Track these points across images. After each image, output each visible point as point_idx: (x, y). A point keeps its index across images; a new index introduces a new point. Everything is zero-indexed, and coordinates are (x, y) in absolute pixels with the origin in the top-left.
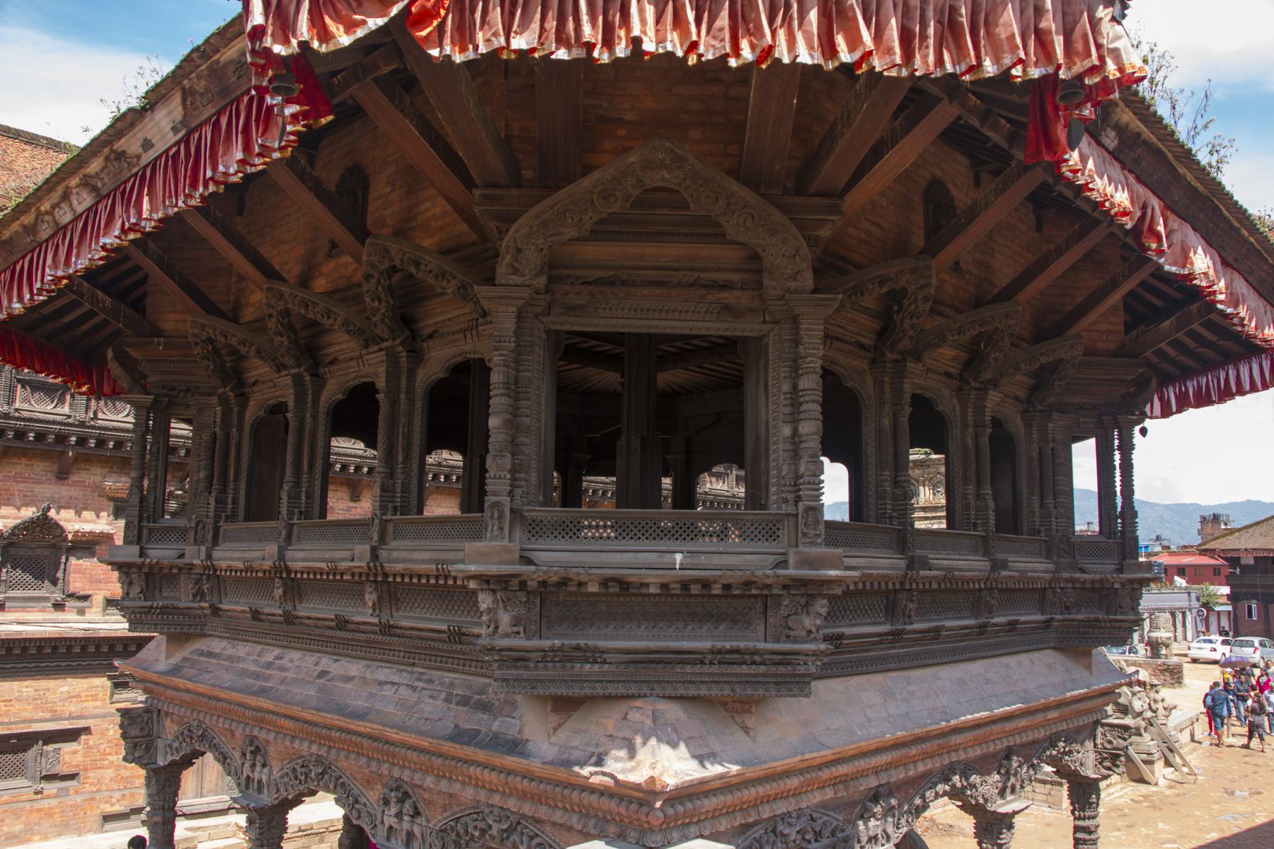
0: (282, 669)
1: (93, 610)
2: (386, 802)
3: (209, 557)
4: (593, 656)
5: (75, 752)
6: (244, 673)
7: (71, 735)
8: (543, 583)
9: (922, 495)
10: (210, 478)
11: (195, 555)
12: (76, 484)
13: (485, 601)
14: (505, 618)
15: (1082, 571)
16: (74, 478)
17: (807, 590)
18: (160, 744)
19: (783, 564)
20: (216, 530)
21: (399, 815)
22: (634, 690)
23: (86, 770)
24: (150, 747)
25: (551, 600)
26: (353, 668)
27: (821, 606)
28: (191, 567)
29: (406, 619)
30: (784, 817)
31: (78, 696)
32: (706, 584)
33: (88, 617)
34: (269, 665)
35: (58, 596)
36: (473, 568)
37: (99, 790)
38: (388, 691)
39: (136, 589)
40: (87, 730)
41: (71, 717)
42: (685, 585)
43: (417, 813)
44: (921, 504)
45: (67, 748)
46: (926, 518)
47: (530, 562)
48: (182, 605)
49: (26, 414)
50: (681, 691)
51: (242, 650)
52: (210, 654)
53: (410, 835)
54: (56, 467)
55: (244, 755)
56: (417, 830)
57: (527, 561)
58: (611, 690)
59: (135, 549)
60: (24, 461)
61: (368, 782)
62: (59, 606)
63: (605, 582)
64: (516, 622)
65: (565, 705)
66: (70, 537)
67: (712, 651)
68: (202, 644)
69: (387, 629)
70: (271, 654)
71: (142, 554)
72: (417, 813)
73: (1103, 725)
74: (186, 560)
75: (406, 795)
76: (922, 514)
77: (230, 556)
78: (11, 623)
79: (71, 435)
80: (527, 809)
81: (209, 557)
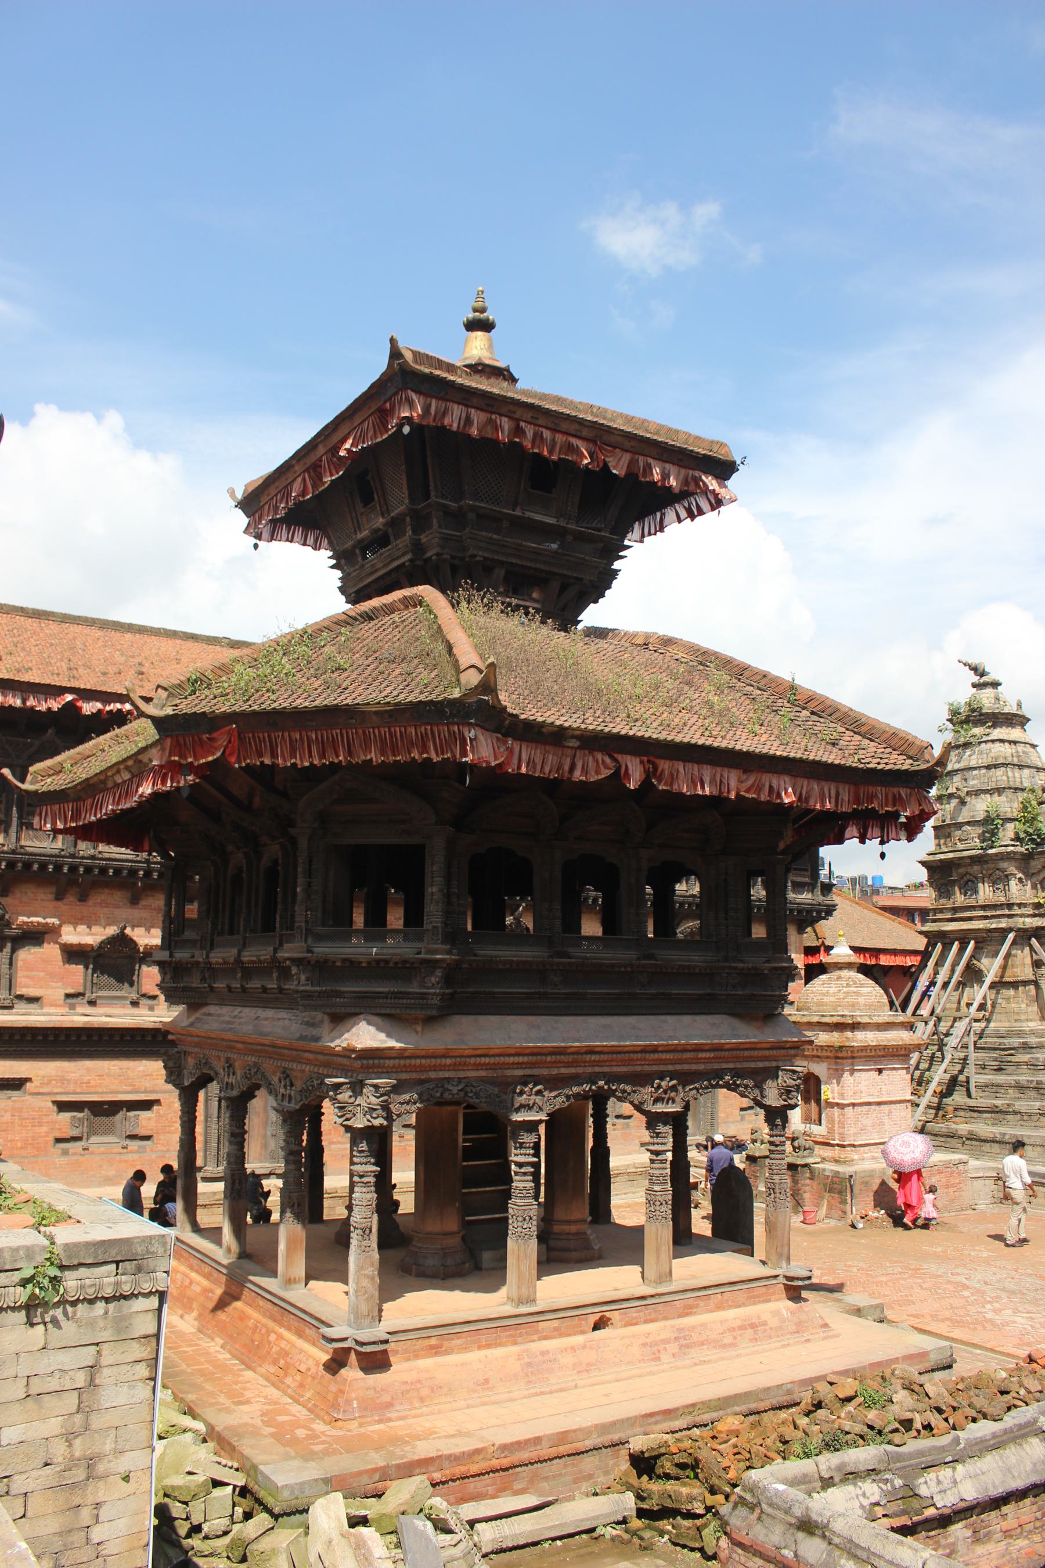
0: (241, 1018)
1: (161, 1007)
3: (207, 957)
4: (340, 994)
5: (149, 1119)
6: (223, 1022)
7: (146, 1105)
8: (317, 962)
9: (981, 892)
11: (200, 956)
12: (145, 907)
14: (303, 977)
15: (742, 961)
16: (143, 903)
17: (431, 965)
18: (185, 1072)
19: (419, 953)
20: (212, 941)
22: (357, 1010)
23: (158, 1133)
24: (180, 1074)
25: (322, 969)
26: (270, 1013)
27: (439, 973)
28: (198, 963)
30: (448, 1080)
31: (151, 1075)
32: (387, 962)
33: (156, 1012)
34: (235, 1017)
35: (134, 996)
36: (286, 955)
37: (168, 1150)
38: (281, 1023)
39: (168, 977)
40: (157, 1102)
41: (145, 1092)
42: (378, 961)
43: (292, 1085)
44: (980, 903)
45: (144, 1115)
46: (986, 918)
47: (312, 952)
48: (194, 985)
49: (107, 855)
50: (378, 1011)
51: (224, 1010)
52: (209, 1015)
53: (290, 1096)
54: (129, 895)
57: (309, 951)
58: (348, 1010)
59: (167, 953)
60: (106, 891)
62: (135, 1004)
63: (344, 960)
64: (308, 979)
66: (141, 949)
67: (389, 992)
68: (205, 1010)
71: (171, 956)
72: (292, 1085)
73: (782, 1070)
74: (195, 959)
75: (288, 1076)
76: (981, 913)
77: (217, 956)
78: (101, 1015)
79: (139, 870)
81: (207, 957)
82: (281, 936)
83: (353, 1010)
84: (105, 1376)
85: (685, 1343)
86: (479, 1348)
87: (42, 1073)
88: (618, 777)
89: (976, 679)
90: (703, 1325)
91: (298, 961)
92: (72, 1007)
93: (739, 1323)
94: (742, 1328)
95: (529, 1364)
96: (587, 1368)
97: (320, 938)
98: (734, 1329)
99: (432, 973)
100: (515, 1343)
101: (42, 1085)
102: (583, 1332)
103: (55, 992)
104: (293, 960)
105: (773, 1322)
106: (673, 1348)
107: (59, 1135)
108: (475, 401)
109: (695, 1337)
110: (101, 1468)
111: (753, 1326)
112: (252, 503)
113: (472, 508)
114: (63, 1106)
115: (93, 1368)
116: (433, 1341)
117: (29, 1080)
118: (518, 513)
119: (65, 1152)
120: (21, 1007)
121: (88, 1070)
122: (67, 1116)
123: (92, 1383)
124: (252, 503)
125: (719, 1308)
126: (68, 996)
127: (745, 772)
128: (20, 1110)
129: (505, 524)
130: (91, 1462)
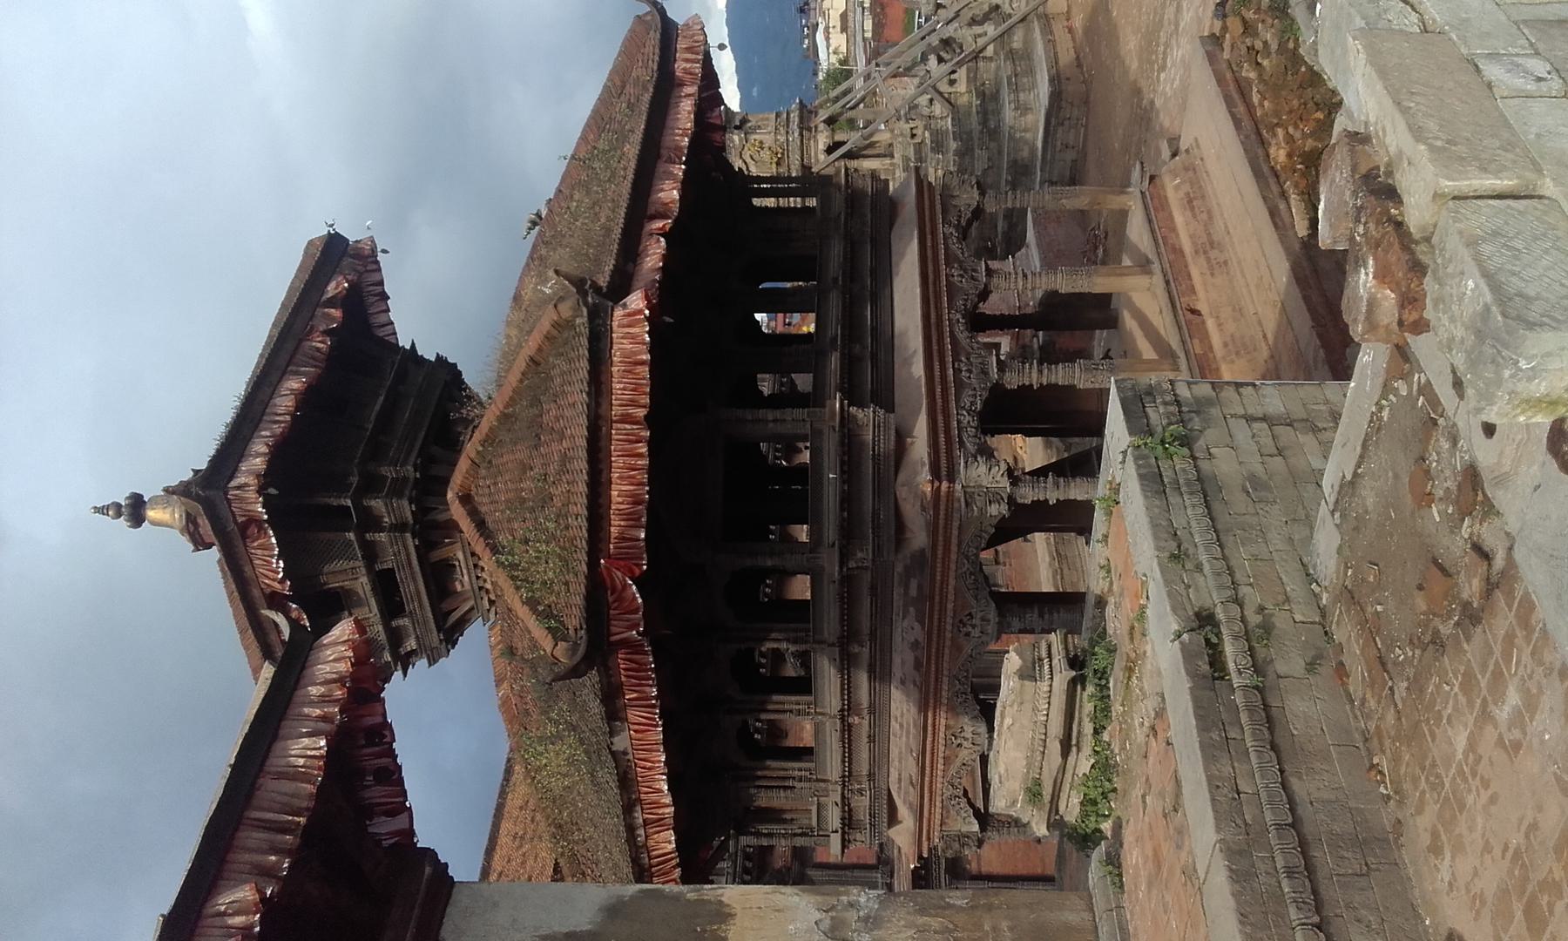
2: (968, 634)
4: (875, 514)
10: (785, 788)
13: (852, 564)
14: (860, 555)
18: (965, 829)
21: (974, 626)
27: (853, 410)
29: (865, 624)
30: (959, 422)
32: (842, 463)
34: (901, 726)
42: (843, 472)
55: (960, 745)
56: (980, 615)
61: (959, 649)
63: (842, 510)
65: (901, 527)
69: (873, 635)
70: (895, 726)
74: (839, 800)
77: (833, 766)
80: (954, 548)
82: (815, 642)
83: (892, 506)
85: (1209, 245)
90: (1191, 237)
93: (1188, 213)
94: (1192, 209)
95: (1237, 353)
96: (1239, 311)
98: (1194, 216)
99: (855, 417)
100: (1218, 369)
102: (1203, 322)
104: (842, 563)
105: (1186, 188)
106: (1213, 254)
109: (1204, 239)
111: (1190, 201)
125: (1174, 229)
127: (659, 156)
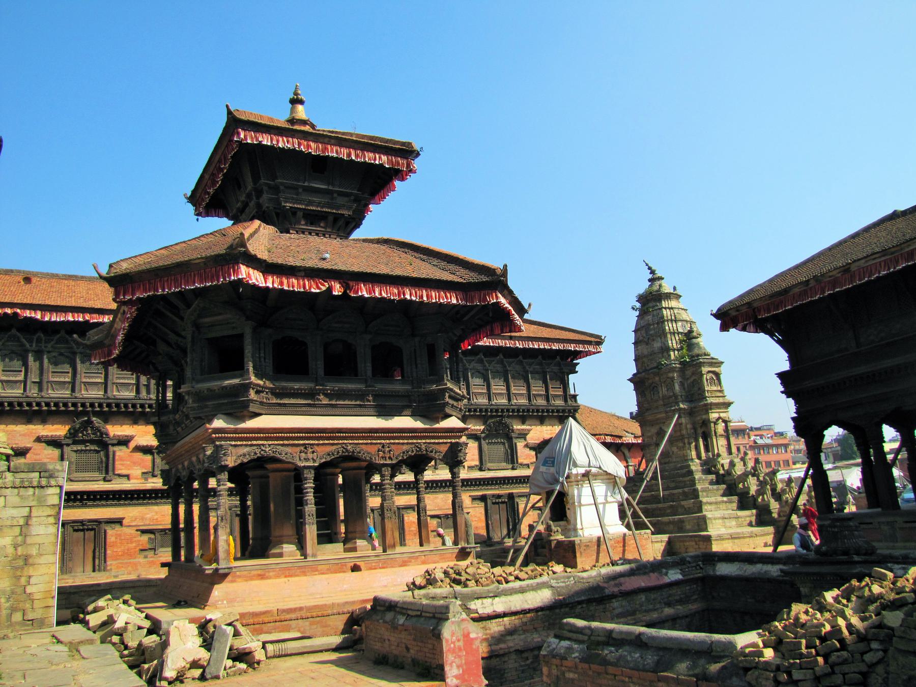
84: (34, 521)
86: (286, 577)
87: (131, 515)
88: (330, 289)
89: (650, 276)
91: (188, 393)
92: (146, 479)
97: (198, 382)
101: (132, 521)
103: (136, 472)
107: (141, 548)
108: (272, 131)
110: (31, 561)
112: (193, 199)
113: (282, 184)
114: (144, 532)
115: (28, 517)
116: (259, 572)
117: (123, 518)
118: (306, 184)
119: (146, 557)
120: (119, 480)
121: (157, 513)
122: (145, 537)
123: (27, 524)
124: (193, 199)
126: (143, 473)
128: (120, 535)
129: (300, 190)
130: (26, 559)
